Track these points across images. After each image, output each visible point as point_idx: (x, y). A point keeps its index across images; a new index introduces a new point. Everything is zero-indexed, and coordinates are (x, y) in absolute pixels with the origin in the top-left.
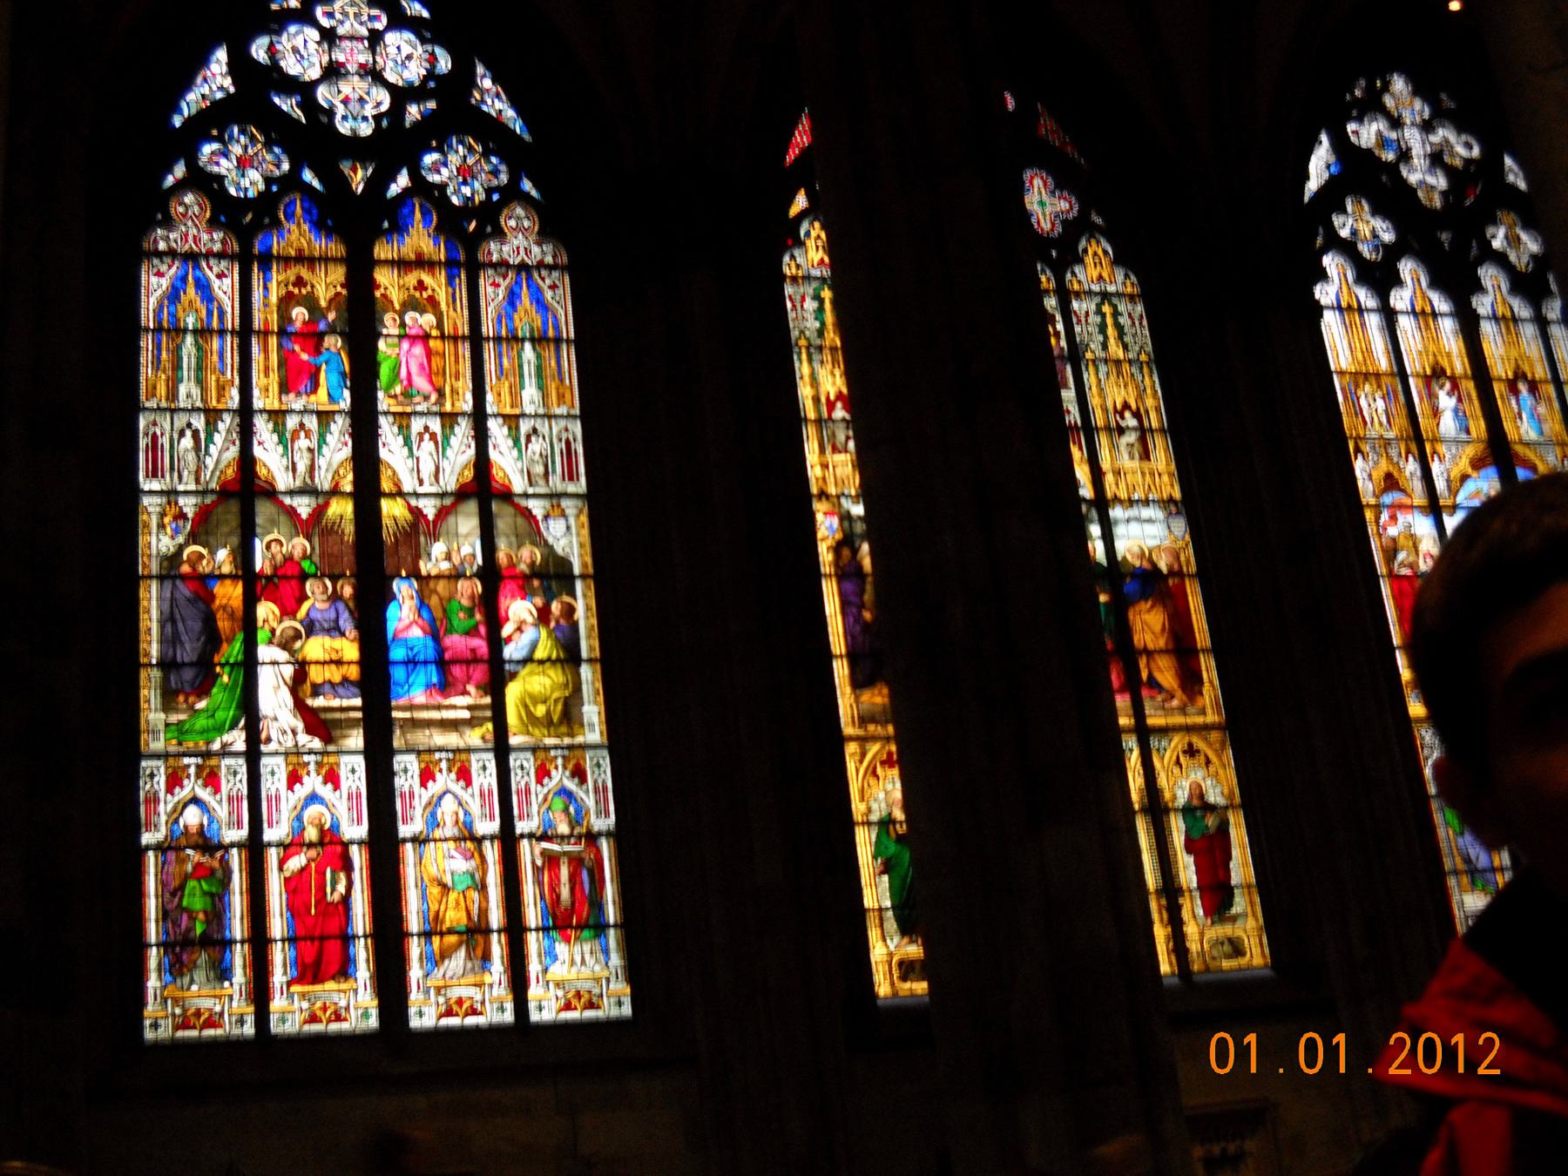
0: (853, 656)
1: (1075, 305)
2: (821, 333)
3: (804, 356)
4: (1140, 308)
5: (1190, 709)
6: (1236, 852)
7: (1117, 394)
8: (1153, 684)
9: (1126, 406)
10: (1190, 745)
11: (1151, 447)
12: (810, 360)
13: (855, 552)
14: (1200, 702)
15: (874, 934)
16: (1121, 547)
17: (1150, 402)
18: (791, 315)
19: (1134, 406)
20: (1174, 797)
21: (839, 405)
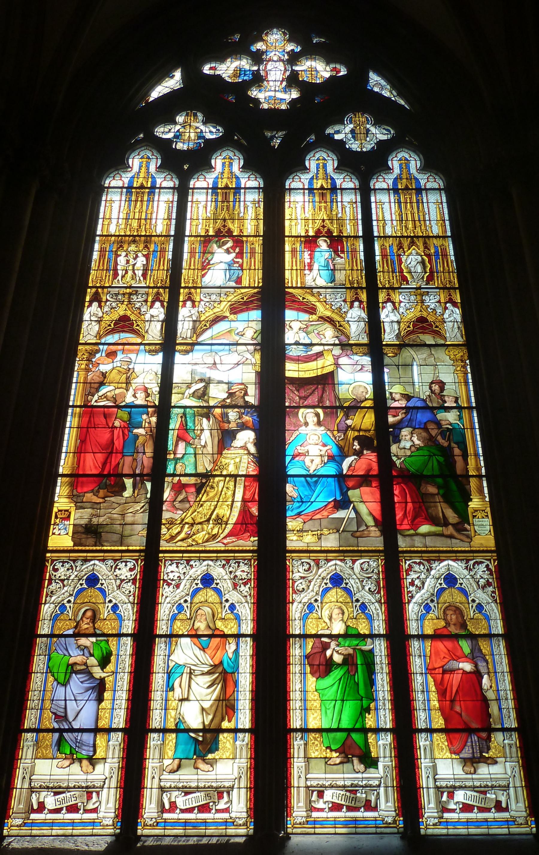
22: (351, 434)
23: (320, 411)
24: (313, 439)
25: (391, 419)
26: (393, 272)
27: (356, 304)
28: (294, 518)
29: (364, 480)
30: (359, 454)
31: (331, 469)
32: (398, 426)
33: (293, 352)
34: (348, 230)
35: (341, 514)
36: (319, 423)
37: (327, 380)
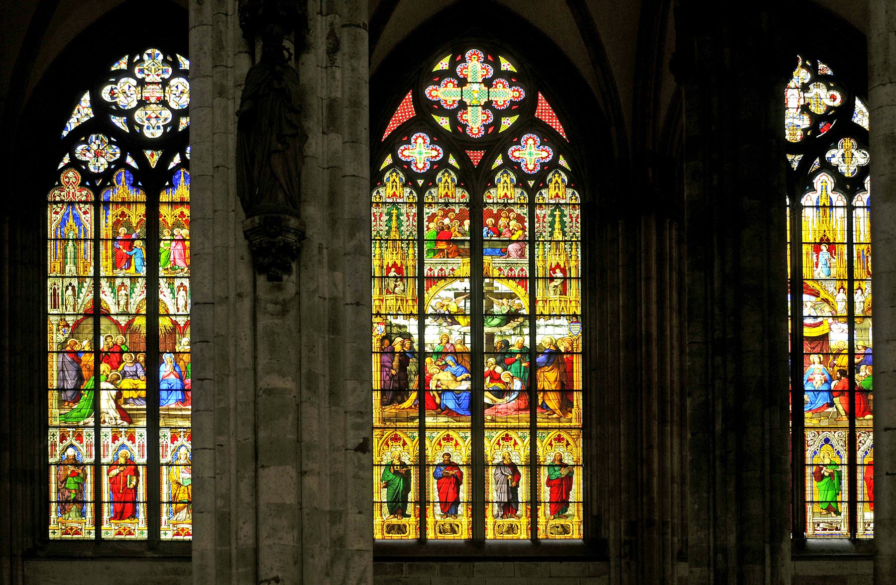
0: (383, 391)
1: (538, 212)
2: (388, 232)
3: (377, 245)
4: (578, 212)
5: (563, 419)
6: (574, 487)
7: (553, 260)
8: (545, 407)
9: (558, 266)
10: (559, 436)
11: (568, 287)
12: (380, 247)
13: (391, 342)
14: (570, 416)
15: (377, 513)
16: (539, 340)
17: (573, 264)
18: (373, 224)
19: (562, 266)
20: (545, 460)
21: (393, 269)
22: (836, 368)
23: (821, 356)
24: (817, 371)
25: (856, 360)
26: (863, 268)
27: (842, 290)
28: (808, 412)
29: (841, 393)
30: (839, 379)
31: (825, 387)
32: (860, 364)
33: (807, 321)
34: (839, 239)
35: (830, 409)
36: (821, 363)
37: (825, 338)
